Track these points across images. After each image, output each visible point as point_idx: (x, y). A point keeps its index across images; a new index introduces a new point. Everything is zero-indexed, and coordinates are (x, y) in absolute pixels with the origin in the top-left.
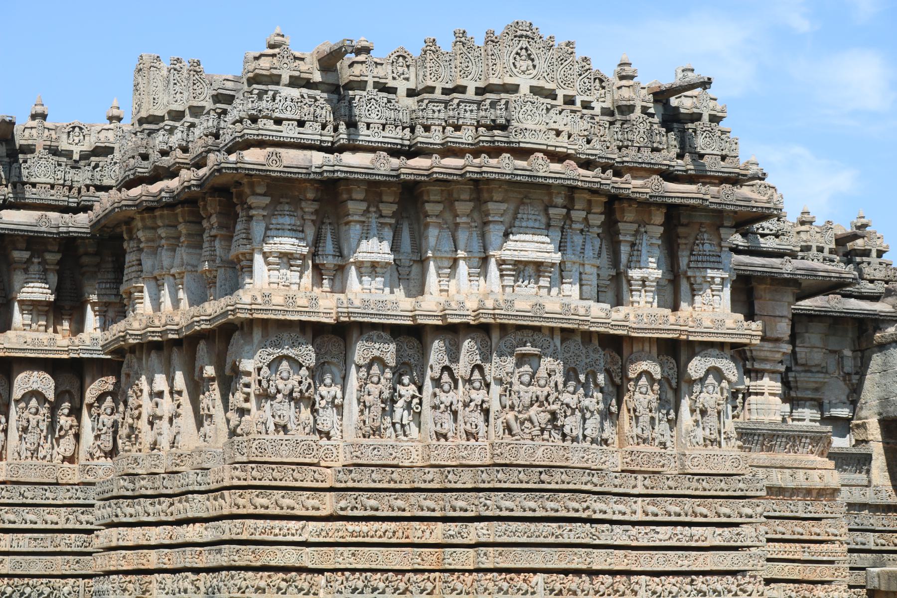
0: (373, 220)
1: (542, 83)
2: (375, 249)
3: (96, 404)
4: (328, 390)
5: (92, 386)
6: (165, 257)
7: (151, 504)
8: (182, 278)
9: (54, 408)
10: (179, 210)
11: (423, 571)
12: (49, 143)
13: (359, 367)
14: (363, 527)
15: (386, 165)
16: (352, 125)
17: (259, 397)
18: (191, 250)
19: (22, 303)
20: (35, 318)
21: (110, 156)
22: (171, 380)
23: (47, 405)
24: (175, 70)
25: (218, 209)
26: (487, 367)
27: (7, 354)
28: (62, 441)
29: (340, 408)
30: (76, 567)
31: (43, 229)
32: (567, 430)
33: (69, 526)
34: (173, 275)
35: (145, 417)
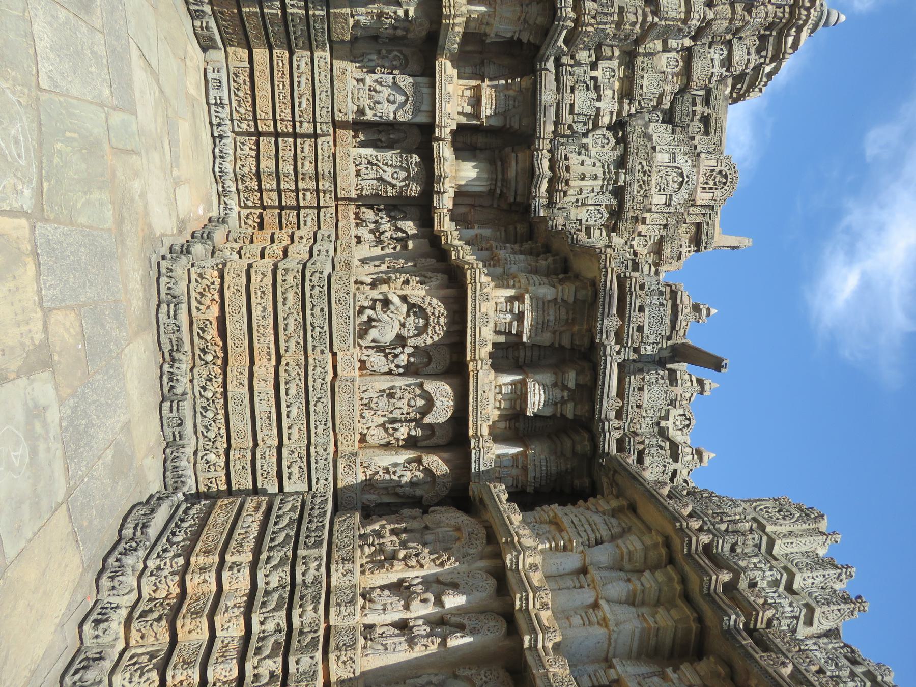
3: (421, 467)
5: (440, 461)
7: (278, 625)
8: (598, 623)
10: (687, 611)
12: (679, 399)
18: (636, 638)
19: (523, 383)
20: (507, 397)
21: (671, 460)
23: (418, 416)
24: (840, 574)
27: (471, 374)
28: (381, 430)
30: (238, 466)
31: (605, 404)
33: (285, 452)
34: (595, 605)
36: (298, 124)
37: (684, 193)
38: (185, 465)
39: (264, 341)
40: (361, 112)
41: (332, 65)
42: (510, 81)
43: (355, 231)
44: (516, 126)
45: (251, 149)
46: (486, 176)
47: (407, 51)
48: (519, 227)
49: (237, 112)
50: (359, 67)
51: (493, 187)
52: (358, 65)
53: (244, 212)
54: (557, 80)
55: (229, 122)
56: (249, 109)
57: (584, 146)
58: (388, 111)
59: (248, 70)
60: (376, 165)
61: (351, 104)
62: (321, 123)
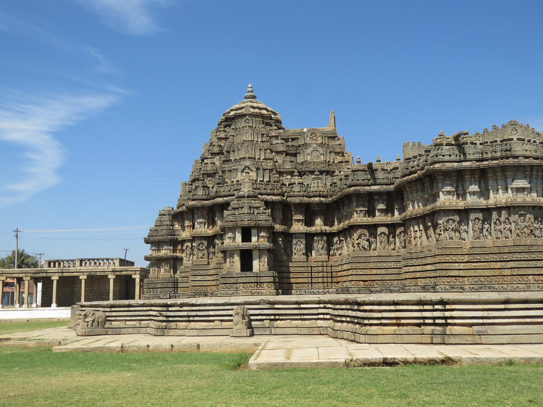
0: (473, 180)
1: (520, 137)
2: (474, 188)
4: (463, 227)
6: (415, 195)
9: (388, 236)
10: (418, 182)
11: (495, 276)
13: (472, 221)
14: (477, 264)
15: (475, 164)
16: (465, 154)
17: (444, 230)
19: (378, 210)
22: (419, 227)
25: (428, 181)
26: (510, 218)
29: (467, 232)
32: (536, 234)
35: (413, 237)
37: (320, 149)
38: (396, 289)
39: (368, 272)
40: (303, 254)
43: (338, 256)
53: (333, 287)
54: (291, 197)
57: (308, 185)
58: (303, 246)
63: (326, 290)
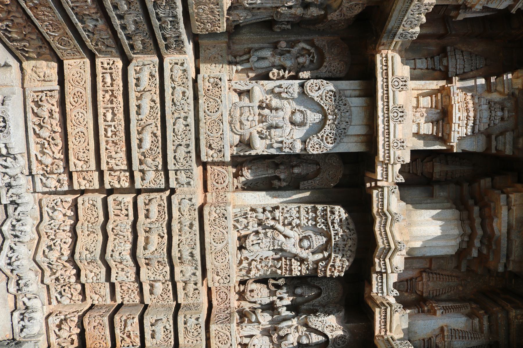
36: (138, 175)
40: (248, 144)
41: (198, 71)
42: (493, 79)
44: (508, 151)
45: (65, 215)
46: (456, 232)
47: (319, 41)
48: (513, 313)
49: (40, 162)
50: (242, 71)
51: (464, 246)
52: (240, 68)
55: (24, 181)
56: (58, 156)
59: (56, 95)
60: (273, 228)
61: (228, 134)
62: (176, 171)
63: (31, 277)
